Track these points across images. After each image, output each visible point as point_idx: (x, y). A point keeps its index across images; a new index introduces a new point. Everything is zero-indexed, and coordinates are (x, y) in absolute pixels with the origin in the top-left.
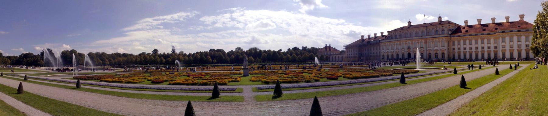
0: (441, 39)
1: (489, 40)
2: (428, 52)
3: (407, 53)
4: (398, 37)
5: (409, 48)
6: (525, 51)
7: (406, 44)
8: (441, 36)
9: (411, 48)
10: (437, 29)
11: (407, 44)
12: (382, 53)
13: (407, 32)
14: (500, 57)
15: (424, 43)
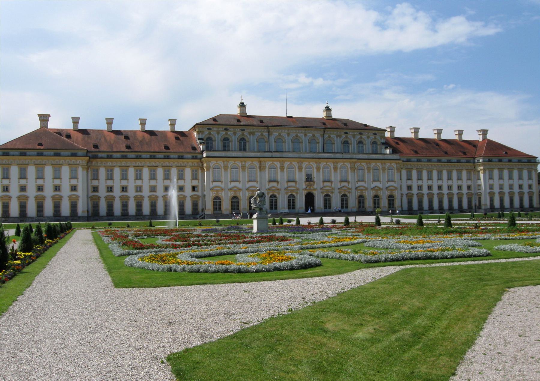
0: (373, 165)
1: (459, 172)
2: (358, 193)
3: (304, 193)
4: (234, 144)
5: (309, 179)
6: (499, 195)
7: (300, 168)
8: (320, 155)
9: (315, 180)
10: (347, 137)
11: (303, 170)
12: (212, 189)
13: (266, 134)
14: (486, 205)
15: (350, 171)
